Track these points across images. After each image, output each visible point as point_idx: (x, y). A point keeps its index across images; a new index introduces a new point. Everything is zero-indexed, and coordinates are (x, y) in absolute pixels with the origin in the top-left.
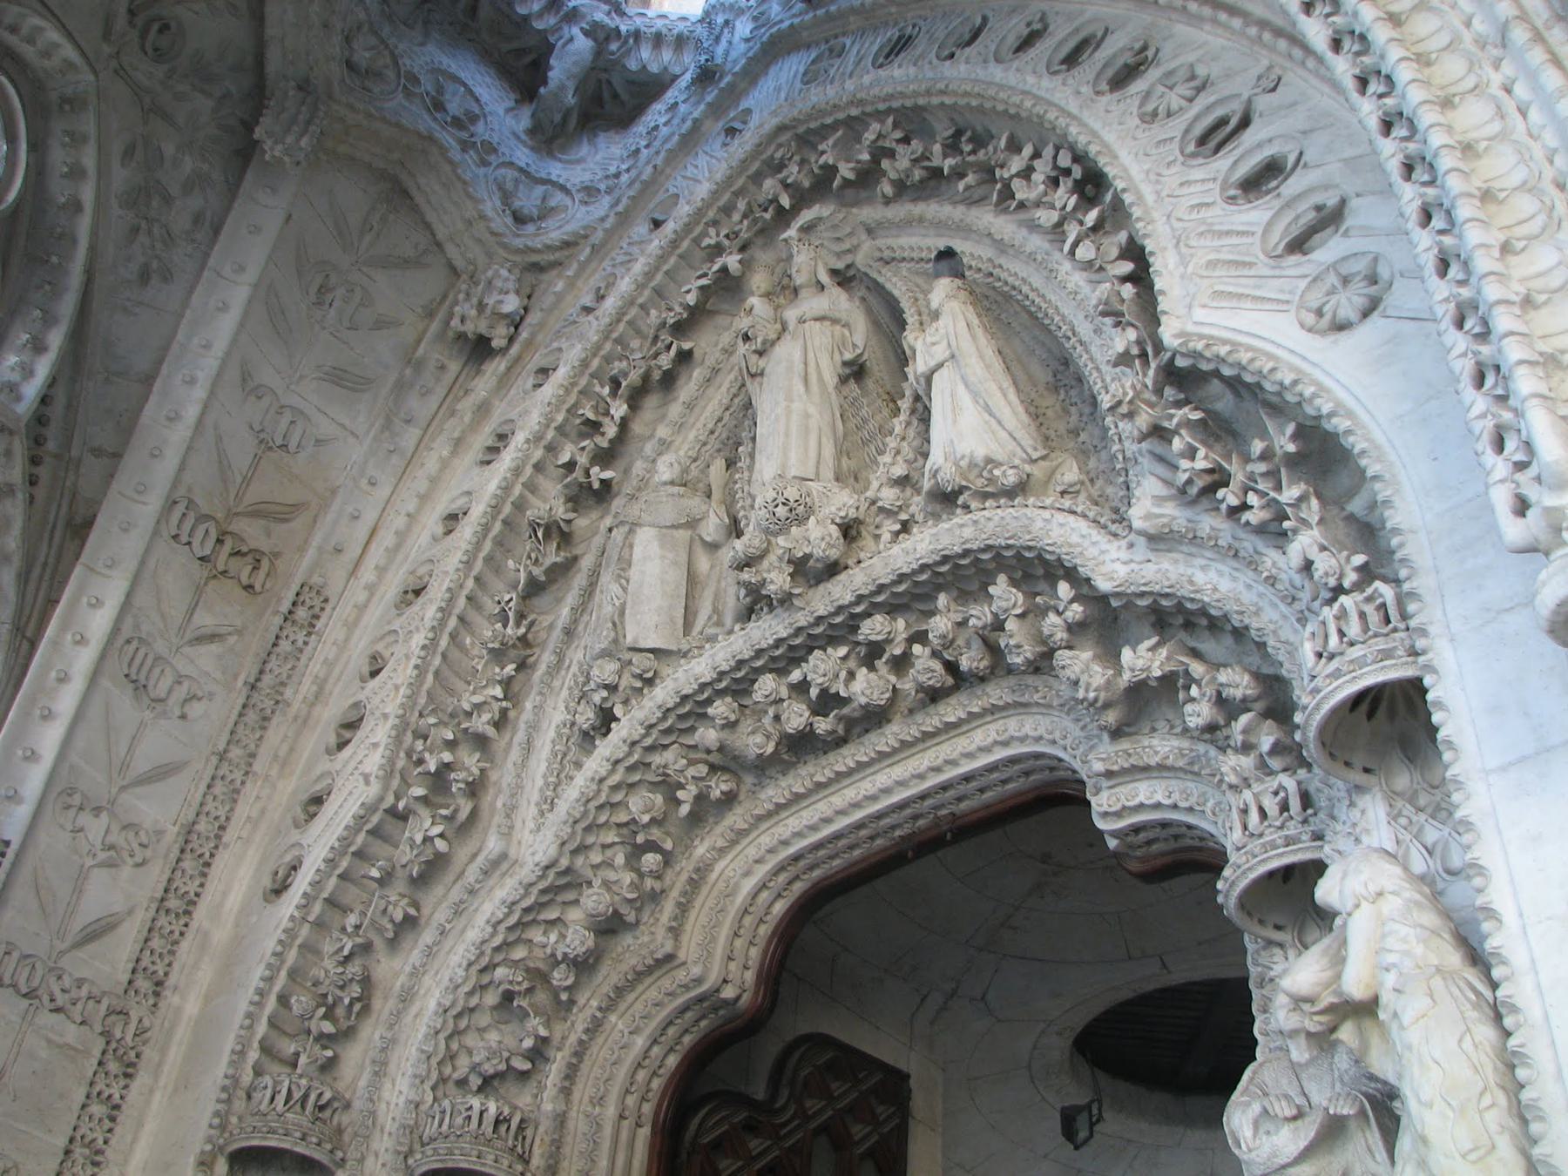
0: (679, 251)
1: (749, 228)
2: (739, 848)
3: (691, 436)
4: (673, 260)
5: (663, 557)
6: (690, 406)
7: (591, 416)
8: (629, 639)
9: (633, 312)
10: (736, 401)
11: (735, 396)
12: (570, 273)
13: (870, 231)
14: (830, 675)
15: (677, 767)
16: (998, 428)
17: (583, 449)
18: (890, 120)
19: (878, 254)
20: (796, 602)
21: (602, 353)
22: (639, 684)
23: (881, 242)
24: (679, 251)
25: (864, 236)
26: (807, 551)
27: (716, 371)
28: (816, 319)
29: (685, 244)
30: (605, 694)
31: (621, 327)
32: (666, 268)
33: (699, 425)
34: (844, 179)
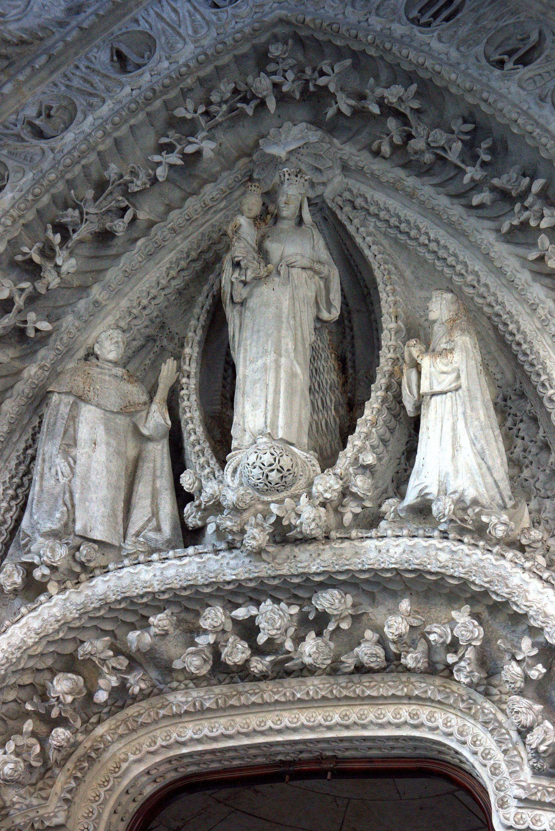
0: (149, 109)
1: (223, 115)
2: (135, 736)
3: (124, 303)
4: (141, 116)
5: (108, 444)
6: (128, 275)
7: (37, 259)
8: (78, 527)
9: (93, 157)
10: (173, 283)
11: (173, 278)
12: (21, 78)
13: (345, 168)
14: (282, 630)
15: (102, 656)
16: (488, 474)
17: (22, 290)
18: (414, 88)
19: (347, 195)
20: (264, 556)
21: (53, 191)
22: (78, 569)
23: (351, 182)
24: (149, 109)
25: (338, 171)
26: (293, 522)
27: (160, 247)
28: (303, 268)
29: (158, 103)
30: (47, 571)
31: (77, 169)
32: (132, 122)
33: (133, 295)
34: (339, 110)
